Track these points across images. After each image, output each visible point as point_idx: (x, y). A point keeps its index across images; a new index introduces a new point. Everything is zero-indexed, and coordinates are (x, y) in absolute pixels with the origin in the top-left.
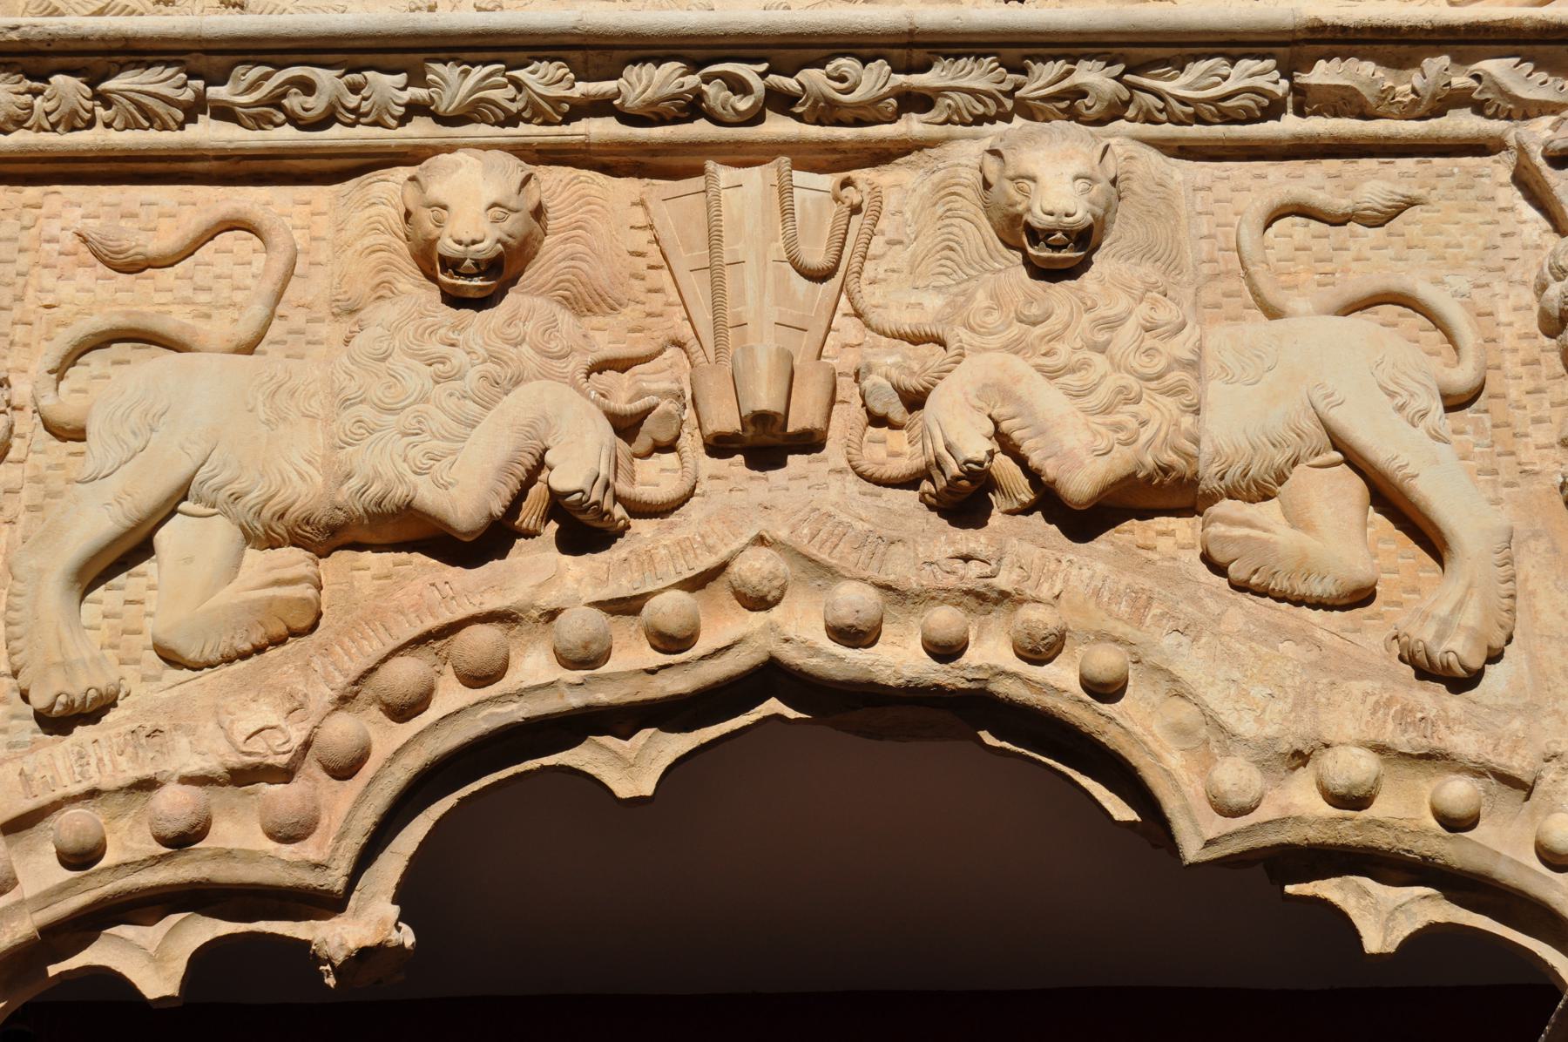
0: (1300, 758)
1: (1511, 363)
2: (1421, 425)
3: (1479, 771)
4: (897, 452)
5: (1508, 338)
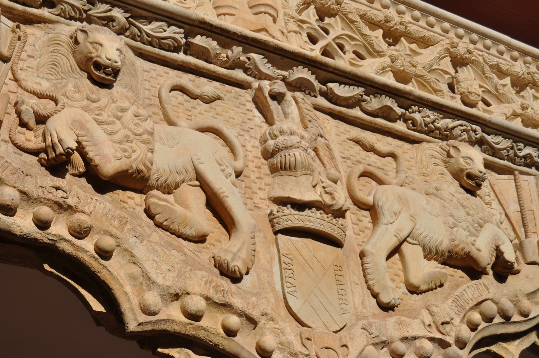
0: (177, 297)
1: (251, 166)
2: (229, 179)
3: (241, 314)
4: (32, 139)
5: (250, 157)
